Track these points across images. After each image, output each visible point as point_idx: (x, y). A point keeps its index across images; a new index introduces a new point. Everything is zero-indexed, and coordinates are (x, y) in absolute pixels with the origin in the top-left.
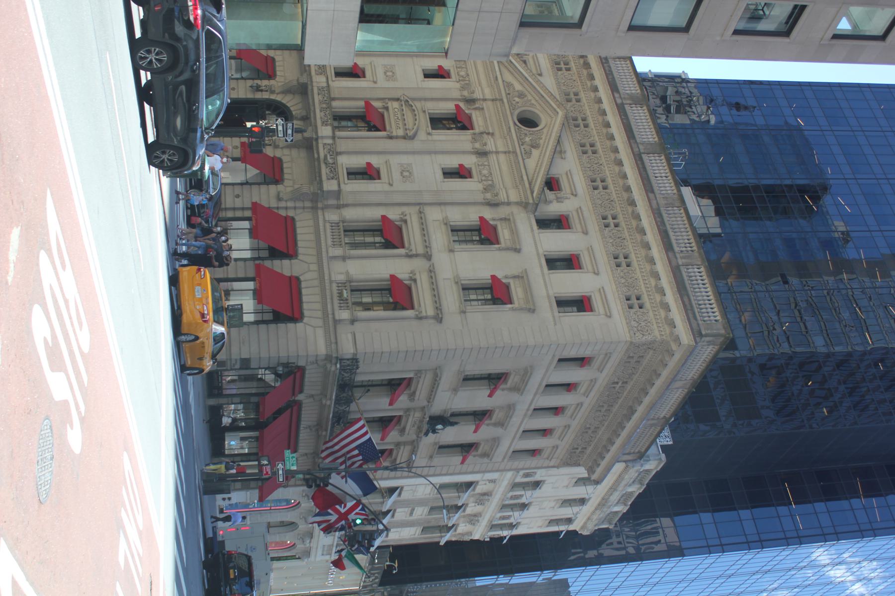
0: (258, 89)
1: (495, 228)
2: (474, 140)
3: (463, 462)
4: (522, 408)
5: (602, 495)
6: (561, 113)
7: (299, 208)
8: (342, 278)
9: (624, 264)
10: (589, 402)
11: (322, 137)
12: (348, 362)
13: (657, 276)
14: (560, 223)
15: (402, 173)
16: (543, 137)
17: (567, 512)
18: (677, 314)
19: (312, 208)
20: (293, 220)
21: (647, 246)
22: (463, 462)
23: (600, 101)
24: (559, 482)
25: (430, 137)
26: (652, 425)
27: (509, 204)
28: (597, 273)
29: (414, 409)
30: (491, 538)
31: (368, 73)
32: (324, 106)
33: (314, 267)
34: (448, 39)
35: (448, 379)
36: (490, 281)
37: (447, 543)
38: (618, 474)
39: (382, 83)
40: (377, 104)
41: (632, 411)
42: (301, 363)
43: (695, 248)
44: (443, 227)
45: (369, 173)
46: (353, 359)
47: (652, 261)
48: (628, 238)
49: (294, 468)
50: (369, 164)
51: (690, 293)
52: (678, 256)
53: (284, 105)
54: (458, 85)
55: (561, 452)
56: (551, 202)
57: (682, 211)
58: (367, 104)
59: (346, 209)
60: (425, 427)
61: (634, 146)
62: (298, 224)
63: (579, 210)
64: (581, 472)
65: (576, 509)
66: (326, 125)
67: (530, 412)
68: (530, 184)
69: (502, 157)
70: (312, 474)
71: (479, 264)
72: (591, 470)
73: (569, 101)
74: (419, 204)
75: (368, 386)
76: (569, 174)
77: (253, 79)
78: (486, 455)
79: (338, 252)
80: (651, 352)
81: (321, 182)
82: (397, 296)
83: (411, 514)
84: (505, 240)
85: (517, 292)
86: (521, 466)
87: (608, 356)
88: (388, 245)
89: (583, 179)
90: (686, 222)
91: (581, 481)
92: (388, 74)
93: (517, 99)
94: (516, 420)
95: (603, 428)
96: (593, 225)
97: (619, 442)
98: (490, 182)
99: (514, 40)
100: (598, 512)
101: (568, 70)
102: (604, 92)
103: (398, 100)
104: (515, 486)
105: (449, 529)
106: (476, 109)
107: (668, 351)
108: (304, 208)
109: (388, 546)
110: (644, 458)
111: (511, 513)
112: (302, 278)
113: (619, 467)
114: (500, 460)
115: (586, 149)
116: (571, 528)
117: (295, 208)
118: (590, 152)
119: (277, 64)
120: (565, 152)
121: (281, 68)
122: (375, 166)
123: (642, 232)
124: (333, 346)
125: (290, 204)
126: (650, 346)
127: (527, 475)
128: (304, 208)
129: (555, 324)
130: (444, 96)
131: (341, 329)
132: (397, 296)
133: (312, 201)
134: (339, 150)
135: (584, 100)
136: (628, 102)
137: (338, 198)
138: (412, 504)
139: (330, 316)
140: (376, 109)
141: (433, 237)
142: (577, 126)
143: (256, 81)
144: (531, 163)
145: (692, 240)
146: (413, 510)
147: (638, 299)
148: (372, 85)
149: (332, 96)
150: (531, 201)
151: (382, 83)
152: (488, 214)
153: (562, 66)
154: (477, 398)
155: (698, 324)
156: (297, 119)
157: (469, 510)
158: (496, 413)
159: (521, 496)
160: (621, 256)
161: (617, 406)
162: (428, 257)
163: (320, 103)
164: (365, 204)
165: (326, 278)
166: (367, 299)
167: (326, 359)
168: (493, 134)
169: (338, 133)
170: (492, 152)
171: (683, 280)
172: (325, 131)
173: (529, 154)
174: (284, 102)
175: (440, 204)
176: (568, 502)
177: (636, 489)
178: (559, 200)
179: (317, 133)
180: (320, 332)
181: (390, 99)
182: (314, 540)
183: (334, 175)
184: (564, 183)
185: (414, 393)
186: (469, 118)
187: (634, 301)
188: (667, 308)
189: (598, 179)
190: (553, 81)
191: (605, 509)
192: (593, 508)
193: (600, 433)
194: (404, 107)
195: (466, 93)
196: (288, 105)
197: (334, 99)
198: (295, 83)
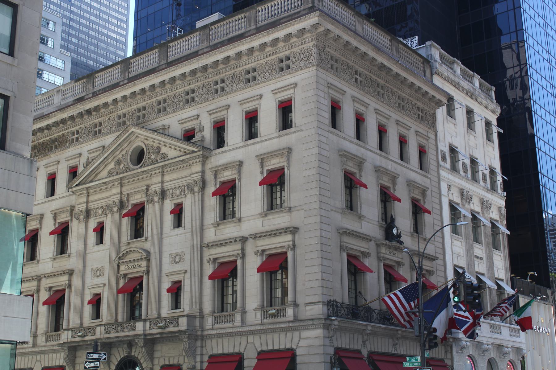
1: (223, 183)
2: (151, 201)
3: (429, 213)
4: (380, 160)
5: (464, 95)
6: (133, 129)
7: (202, 351)
8: (259, 314)
9: (254, 74)
10: (373, 104)
12: (331, 309)
13: (263, 46)
14: (220, 129)
15: (177, 263)
16: (151, 143)
17: (480, 126)
18: (294, 28)
19: (202, 340)
20: (211, 357)
21: (239, 55)
22: (429, 213)
23: (124, 98)
24: (450, 131)
25: (149, 239)
26: (398, 52)
27: (203, 172)
28: (261, 97)
29: (378, 253)
30: (504, 191)
31: (97, 291)
32: (119, 328)
33: (250, 339)
34: (14, 213)
35: (350, 224)
36: (265, 186)
37: (508, 228)
38: (443, 82)
39: (105, 279)
40: (121, 284)
41: (382, 67)
42: (331, 351)
43: (243, 15)
44: (221, 227)
45: (176, 290)
46: (328, 305)
47: (251, 51)
48: (233, 71)
49: (419, 358)
51: (278, 18)
52: (248, 29)
53: (119, 363)
54: (109, 215)
55: (422, 129)
56: (203, 137)
57: (213, 27)
58: (119, 291)
59: (204, 310)
60: (394, 244)
61: (161, 68)
62: (215, 352)
63: (210, 113)
64: (441, 112)
65: (477, 118)
66: (135, 327)
67: (383, 154)
68: (187, 154)
69: (167, 178)
70: (425, 341)
71: (251, 196)
72: (439, 104)
73: (124, 123)
74: (202, 248)
75: (356, 291)
76: (181, 122)
78: (424, 192)
79: (238, 317)
80: (327, 49)
81: (180, 332)
82: (275, 266)
83: (481, 258)
84: (232, 175)
85: (274, 164)
86: (435, 164)
87: (330, 86)
88: (234, 273)
89: (186, 110)
90: (222, 24)
91: (450, 112)
92: (98, 274)
93: (122, 166)
94: (391, 166)
95: (399, 92)
96: (222, 101)
97: (411, 79)
98: (186, 188)
99: (17, 154)
100: (479, 99)
101: (100, 124)
102: (118, 94)
103: (118, 266)
104: (454, 169)
105: (494, 226)
106: (128, 200)
107: (326, 35)
108: (202, 347)
109: (512, 279)
110: (429, 59)
111: (480, 173)
112: (259, 349)
113: (437, 81)
114: (428, 181)
115: (162, 108)
116: (494, 122)
117: (202, 355)
118: (164, 105)
120: (164, 125)
122: (170, 285)
123: (228, 59)
124: (315, 322)
125: (198, 359)
126: (321, 50)
127: (444, 159)
128: (202, 347)
129: (301, 130)
130: (117, 226)
131: (302, 316)
132: (275, 266)
133: (196, 340)
134: (156, 316)
135: (124, 111)
136: (127, 74)
137: (195, 317)
138: (471, 258)
139: (291, 325)
140: (126, 284)
141: (229, 236)
142: (144, 115)
144: (172, 153)
145: (236, 18)
146: (477, 257)
147: (282, 61)
149: (113, 321)
150: (201, 153)
151: (105, 279)
152: (211, 189)
153: (97, 129)
154: (369, 198)
155: (304, 10)
156: (130, 352)
157: (478, 208)
158: (383, 182)
159: (464, 164)
160: (247, 76)
161: (379, 80)
162: (244, 240)
163: (117, 332)
164: (200, 294)
165: (259, 328)
166: (279, 293)
167: (328, 329)
168: (148, 186)
170: (162, 186)
171: (268, 24)
173: (165, 155)
174: (116, 363)
175: (202, 230)
176: (470, 125)
177: (459, 67)
178: (201, 130)
179: (140, 335)
180: (305, 334)
181: (118, 272)
182: (505, 344)
183: (174, 320)
184: (188, 126)
185: (362, 252)
186: (135, 205)
187: (284, 65)
188: (289, 36)
189: (186, 97)
190: (109, 136)
191: (477, 93)
192: (476, 103)
193: (404, 95)
194: (124, 261)
195: (115, 209)
196: (119, 359)
197: (116, 320)
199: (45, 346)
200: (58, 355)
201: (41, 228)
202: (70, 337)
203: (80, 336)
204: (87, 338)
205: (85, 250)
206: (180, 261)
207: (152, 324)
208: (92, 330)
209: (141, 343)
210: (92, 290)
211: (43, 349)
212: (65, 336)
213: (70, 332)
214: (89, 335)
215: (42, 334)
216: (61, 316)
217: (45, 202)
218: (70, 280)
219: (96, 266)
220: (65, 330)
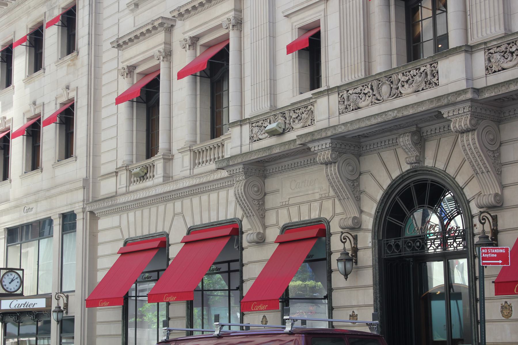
0: (351, 258)
31: (307, 18)
32: (385, 89)
53: (387, 195)
119: (295, 219)
121: (304, 208)
143: (334, 265)
156: (420, 159)
169: (454, 42)
172: (452, 74)
174: (379, 195)
196: (386, 183)
198: (333, 169)
199: (192, 176)
200: (223, 194)
203: (273, 133)
207: (497, 56)
208: (302, 110)
209: (461, 119)
210: (295, 18)
212: (237, 141)
213: (246, 128)
214: (297, 125)
215: (181, 151)
216: (225, 105)
220: (234, 124)
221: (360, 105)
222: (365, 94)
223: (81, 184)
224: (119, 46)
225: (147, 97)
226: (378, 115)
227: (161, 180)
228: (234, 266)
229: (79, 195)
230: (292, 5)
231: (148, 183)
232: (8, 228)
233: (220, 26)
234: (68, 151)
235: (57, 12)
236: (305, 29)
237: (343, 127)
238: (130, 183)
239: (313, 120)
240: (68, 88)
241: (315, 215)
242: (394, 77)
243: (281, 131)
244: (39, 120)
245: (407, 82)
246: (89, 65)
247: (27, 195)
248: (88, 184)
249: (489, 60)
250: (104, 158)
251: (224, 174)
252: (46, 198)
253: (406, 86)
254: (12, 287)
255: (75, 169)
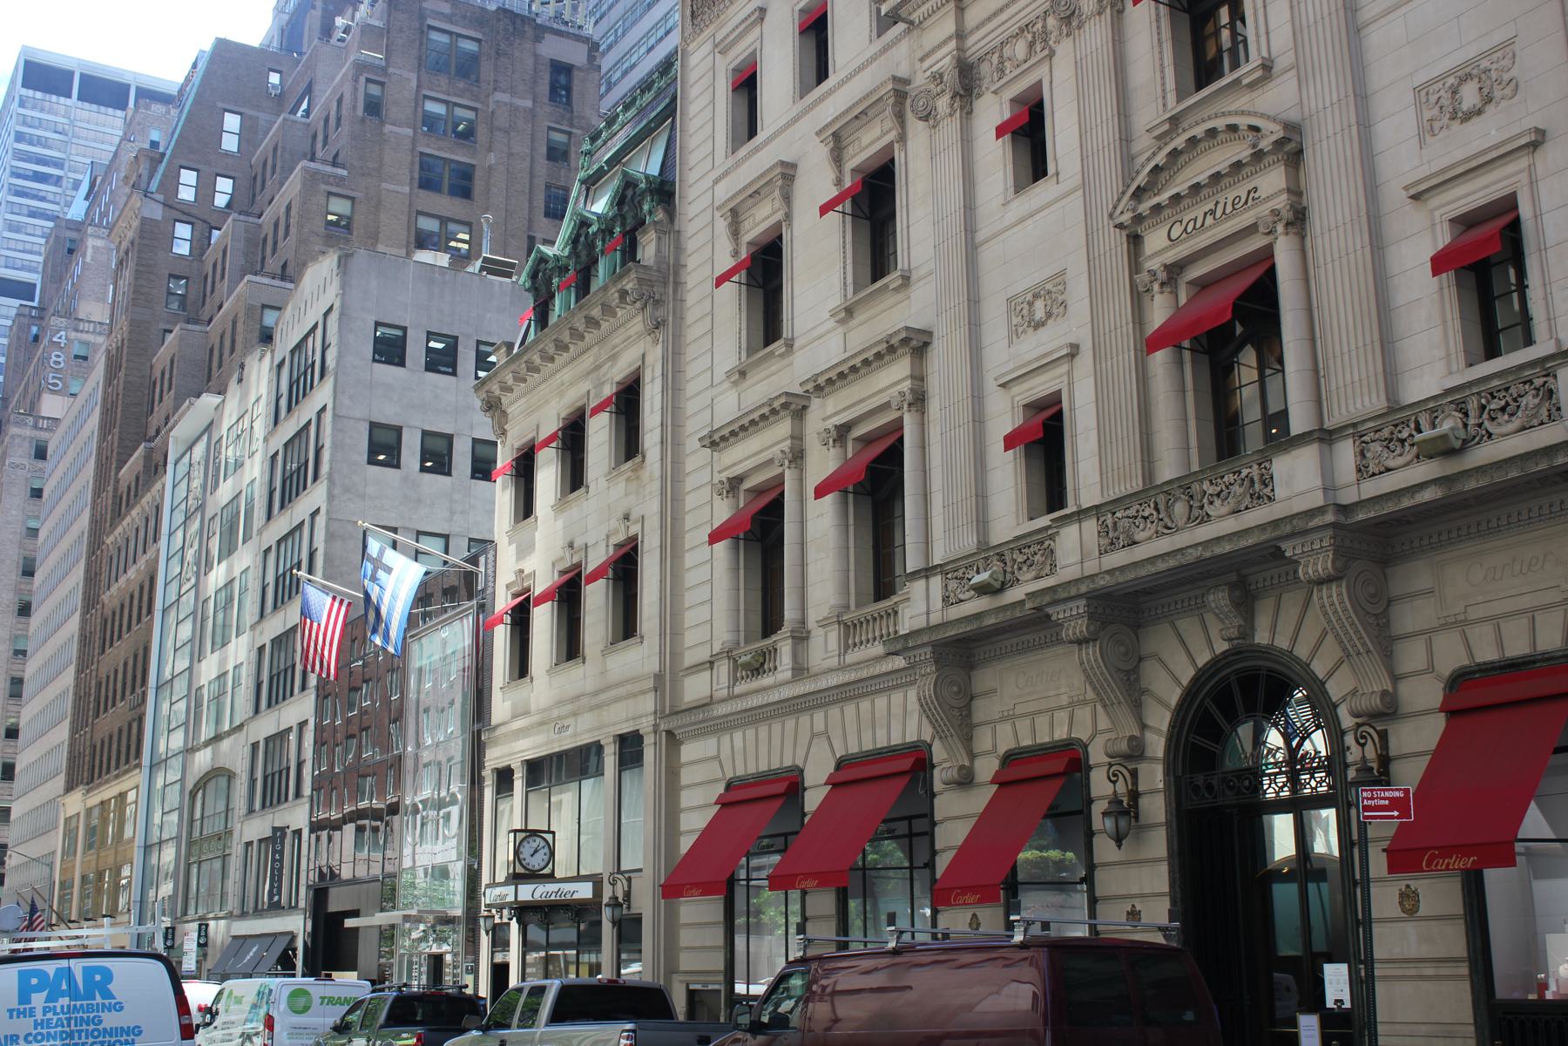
0: (1127, 810)
11: (1329, 488)
15: (1468, 117)
25: (1280, 64)
31: (1040, 387)
32: (1180, 508)
39: (1074, 326)
40: (1159, 313)
50: (1440, 263)
53: (1190, 694)
54: (1064, 49)
58: (1154, 343)
77: (1090, 834)
119: (1026, 742)
121: (1042, 722)
143: (1097, 822)
148: (1085, 361)
151: (1074, 326)
156: (1248, 630)
169: (1298, 425)
172: (1297, 479)
174: (1174, 697)
181: (1135, 264)
196: (1187, 674)
198: (1092, 652)
199: (842, 668)
200: (897, 697)
201: (788, 216)
202: (937, 603)
203: (983, 590)
204: (1015, 594)
205: (970, 228)
206: (1488, 100)
208: (1036, 548)
209: (1316, 560)
210: (1016, 389)
211: (834, 680)
212: (920, 605)
213: (936, 582)
214: (1026, 575)
215: (823, 624)
217: (795, 120)
218: (919, 378)
219: (1025, 280)
220: (915, 575)
221: (1137, 537)
222: (1145, 518)
223: (650, 684)
224: (713, 444)
225: (760, 532)
226: (1168, 554)
227: (788, 674)
228: (920, 826)
229: (648, 703)
230: (1011, 366)
231: (767, 680)
232: (528, 762)
233: (885, 407)
234: (627, 626)
235: (608, 390)
236: (1034, 407)
237: (1107, 577)
238: (736, 680)
239: (1053, 565)
240: (627, 517)
241: (1061, 734)
242: (1196, 487)
243: (997, 585)
244: (579, 574)
245: (1218, 495)
246: (663, 478)
247: (560, 703)
248: (664, 683)
249: (1363, 455)
250: (690, 638)
251: (899, 662)
252: (591, 709)
253: (1217, 502)
254: (536, 862)
255: (640, 657)
